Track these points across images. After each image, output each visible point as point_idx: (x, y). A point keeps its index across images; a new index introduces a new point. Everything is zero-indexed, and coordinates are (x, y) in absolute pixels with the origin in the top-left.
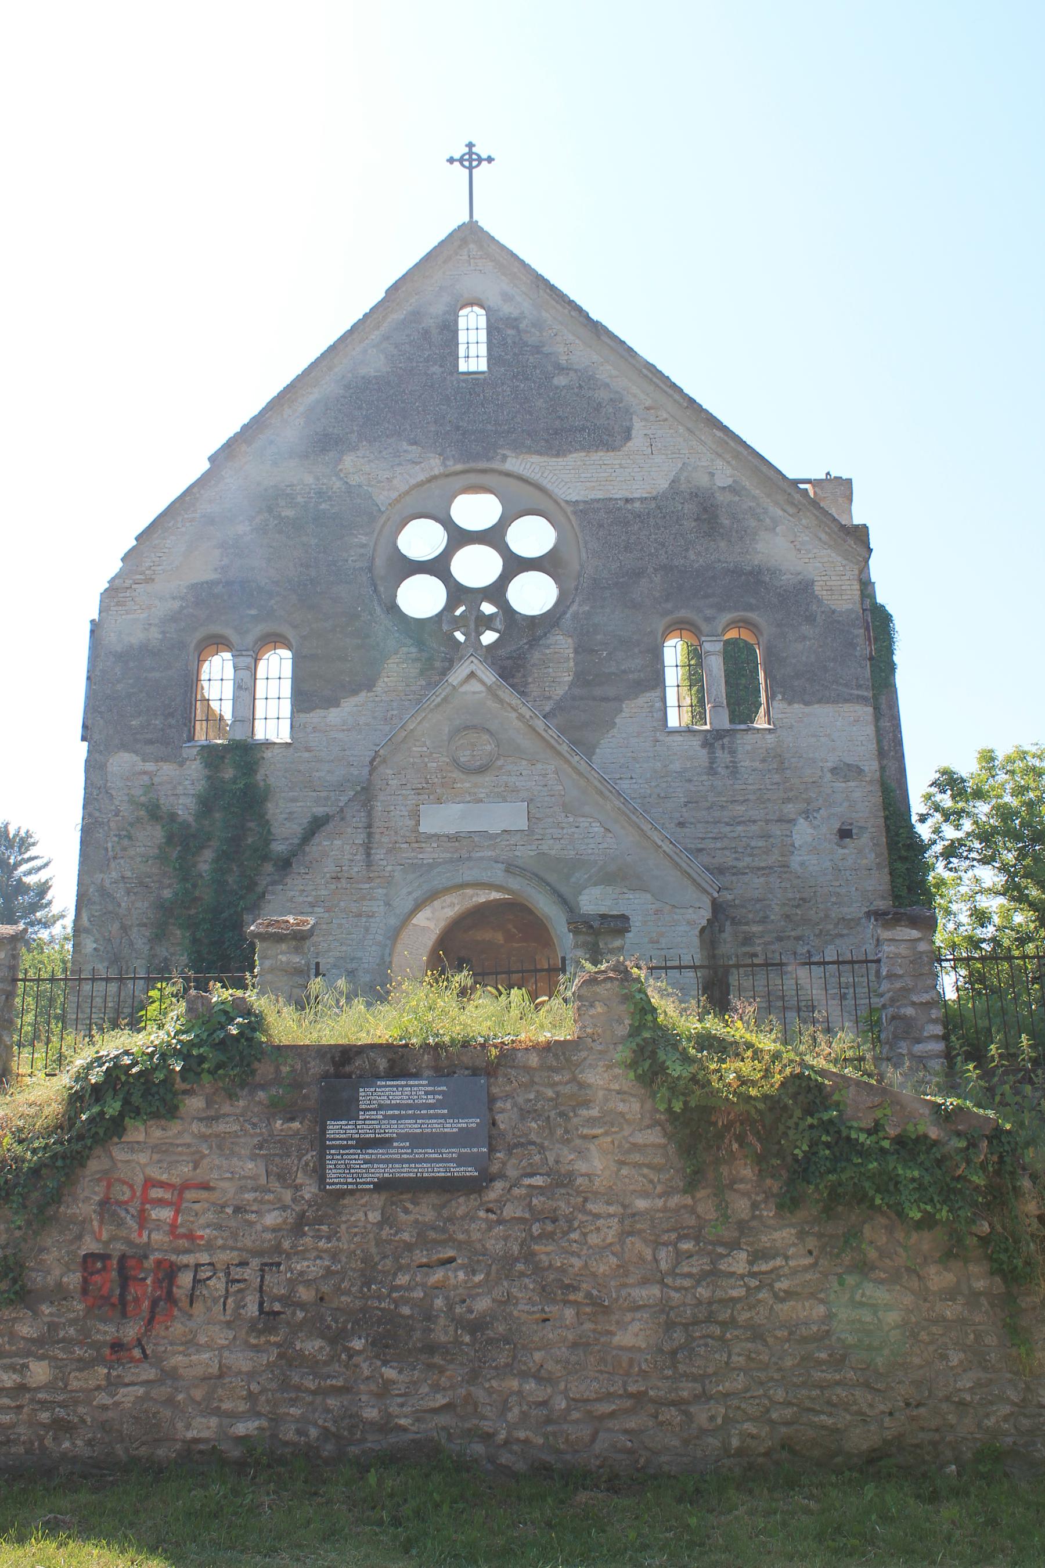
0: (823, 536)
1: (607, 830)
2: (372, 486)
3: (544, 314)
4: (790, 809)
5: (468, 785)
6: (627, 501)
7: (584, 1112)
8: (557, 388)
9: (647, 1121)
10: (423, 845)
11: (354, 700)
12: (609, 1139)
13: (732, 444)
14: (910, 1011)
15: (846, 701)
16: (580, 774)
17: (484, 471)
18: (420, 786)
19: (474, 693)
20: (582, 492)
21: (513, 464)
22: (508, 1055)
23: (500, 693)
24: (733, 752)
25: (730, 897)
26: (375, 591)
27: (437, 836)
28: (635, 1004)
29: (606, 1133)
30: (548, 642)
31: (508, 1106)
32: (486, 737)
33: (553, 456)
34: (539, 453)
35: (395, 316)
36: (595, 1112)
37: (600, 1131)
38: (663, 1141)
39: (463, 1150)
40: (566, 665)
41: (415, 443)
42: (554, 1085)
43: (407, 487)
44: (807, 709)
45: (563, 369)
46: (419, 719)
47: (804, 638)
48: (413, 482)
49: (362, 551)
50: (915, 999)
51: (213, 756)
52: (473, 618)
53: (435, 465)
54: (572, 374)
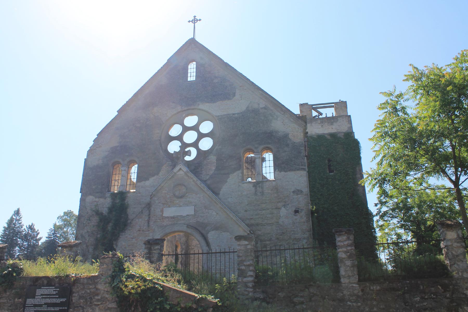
0: (292, 120)
1: (217, 214)
4: (280, 205)
6: (233, 114)
7: (96, 297)
9: (113, 301)
11: (153, 178)
12: (102, 306)
13: (264, 94)
14: (243, 268)
15: (298, 170)
16: (210, 197)
17: (193, 109)
22: (77, 280)
23: (188, 174)
24: (262, 188)
25: (260, 233)
26: (161, 146)
27: (168, 217)
28: (114, 265)
29: (101, 304)
31: (77, 295)
32: (183, 187)
34: (208, 102)
36: (99, 297)
37: (99, 303)
38: (116, 307)
39: (61, 308)
42: (90, 289)
44: (286, 173)
47: (285, 151)
50: (245, 263)
51: (114, 195)
53: (179, 108)
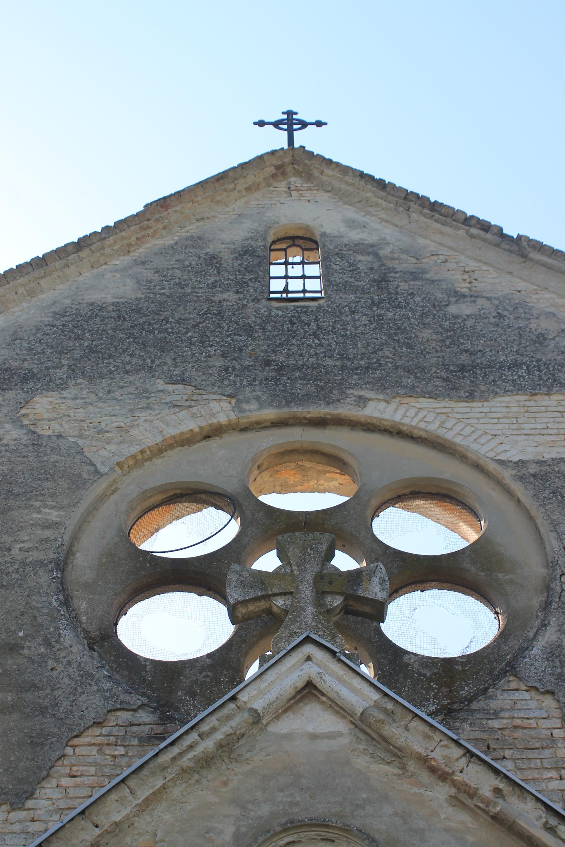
2: (86, 437)
3: (421, 241)
8: (456, 317)
17: (320, 423)
19: (314, 737)
20: (530, 450)
21: (379, 409)
23: (393, 731)
30: (494, 704)
33: (460, 399)
34: (433, 396)
35: (160, 242)
40: (547, 753)
41: (182, 381)
43: (159, 439)
45: (464, 296)
46: (143, 794)
48: (174, 432)
49: (48, 533)
52: (309, 577)
54: (480, 301)
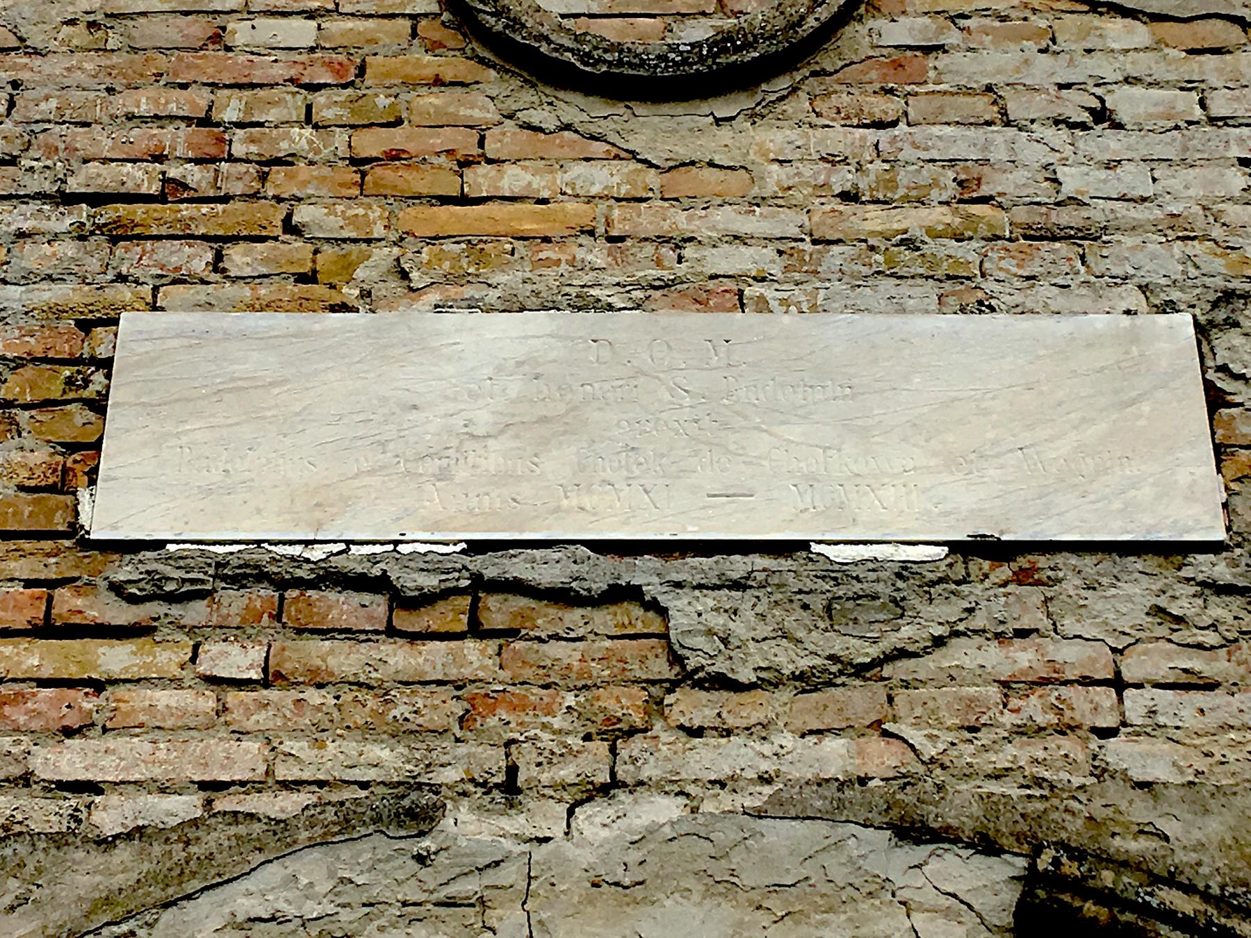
5: (603, 177)
10: (114, 658)
18: (142, 178)
27: (279, 583)
